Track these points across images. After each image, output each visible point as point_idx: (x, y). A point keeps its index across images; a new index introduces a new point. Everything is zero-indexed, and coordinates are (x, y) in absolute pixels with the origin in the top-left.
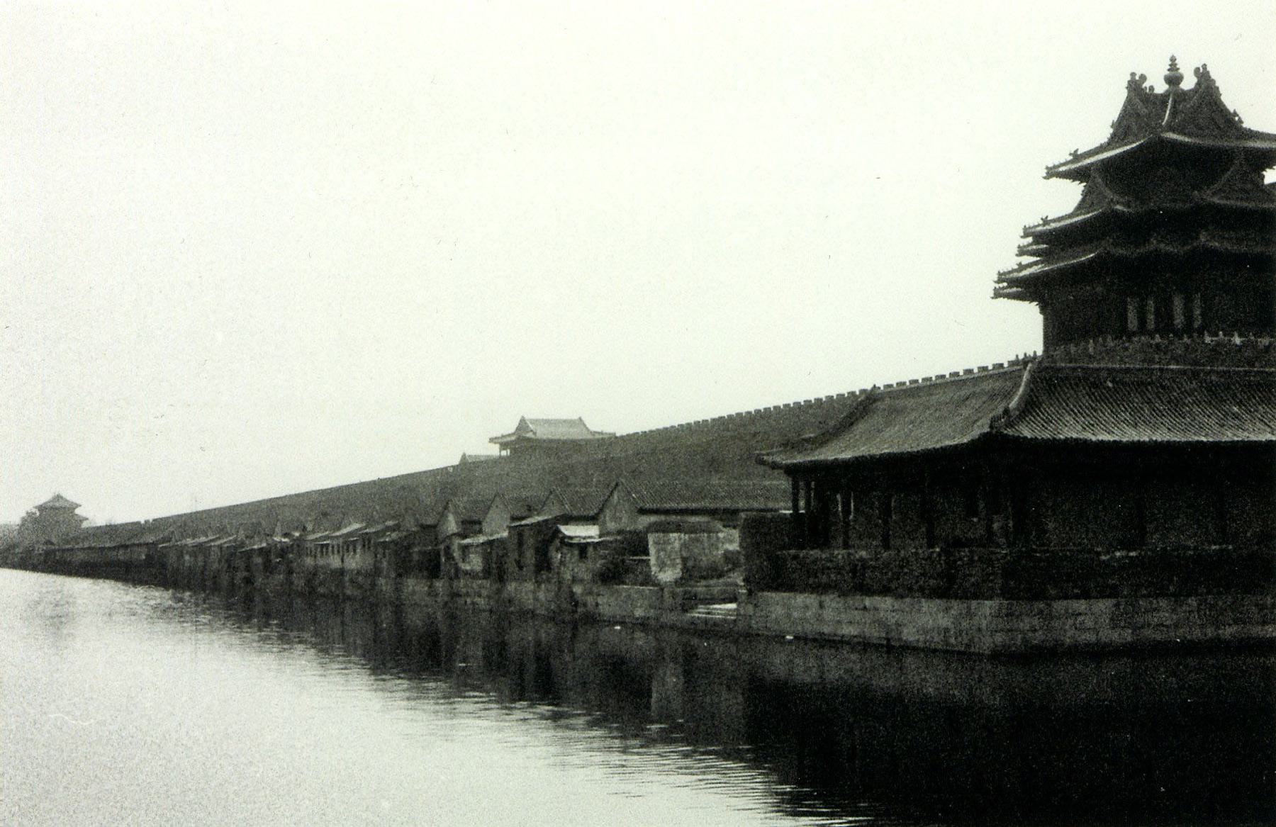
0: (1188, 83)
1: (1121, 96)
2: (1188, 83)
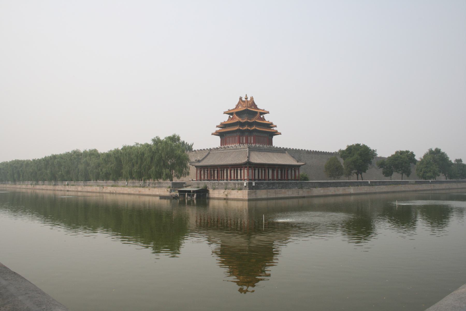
0: (249, 99)
2: (249, 99)
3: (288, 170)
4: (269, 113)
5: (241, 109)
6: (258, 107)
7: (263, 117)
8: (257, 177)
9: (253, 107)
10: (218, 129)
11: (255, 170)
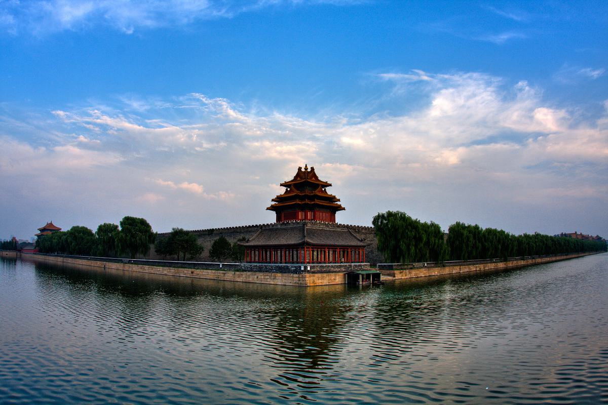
0: (309, 170)
1: (297, 171)
3: (351, 252)
4: (330, 185)
5: (299, 180)
6: (319, 179)
7: (325, 190)
8: (315, 257)
9: (314, 179)
10: (273, 203)
11: (313, 251)
